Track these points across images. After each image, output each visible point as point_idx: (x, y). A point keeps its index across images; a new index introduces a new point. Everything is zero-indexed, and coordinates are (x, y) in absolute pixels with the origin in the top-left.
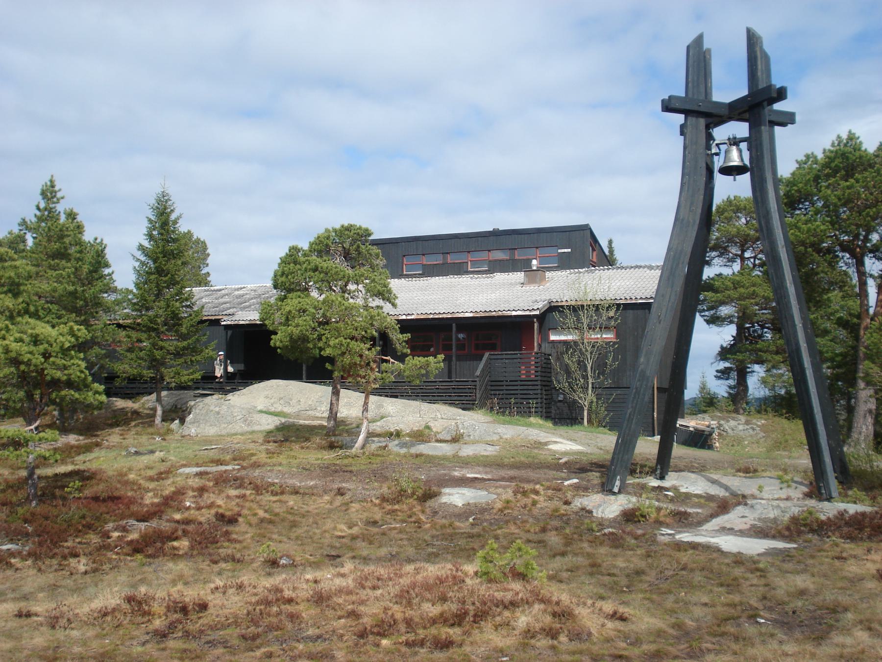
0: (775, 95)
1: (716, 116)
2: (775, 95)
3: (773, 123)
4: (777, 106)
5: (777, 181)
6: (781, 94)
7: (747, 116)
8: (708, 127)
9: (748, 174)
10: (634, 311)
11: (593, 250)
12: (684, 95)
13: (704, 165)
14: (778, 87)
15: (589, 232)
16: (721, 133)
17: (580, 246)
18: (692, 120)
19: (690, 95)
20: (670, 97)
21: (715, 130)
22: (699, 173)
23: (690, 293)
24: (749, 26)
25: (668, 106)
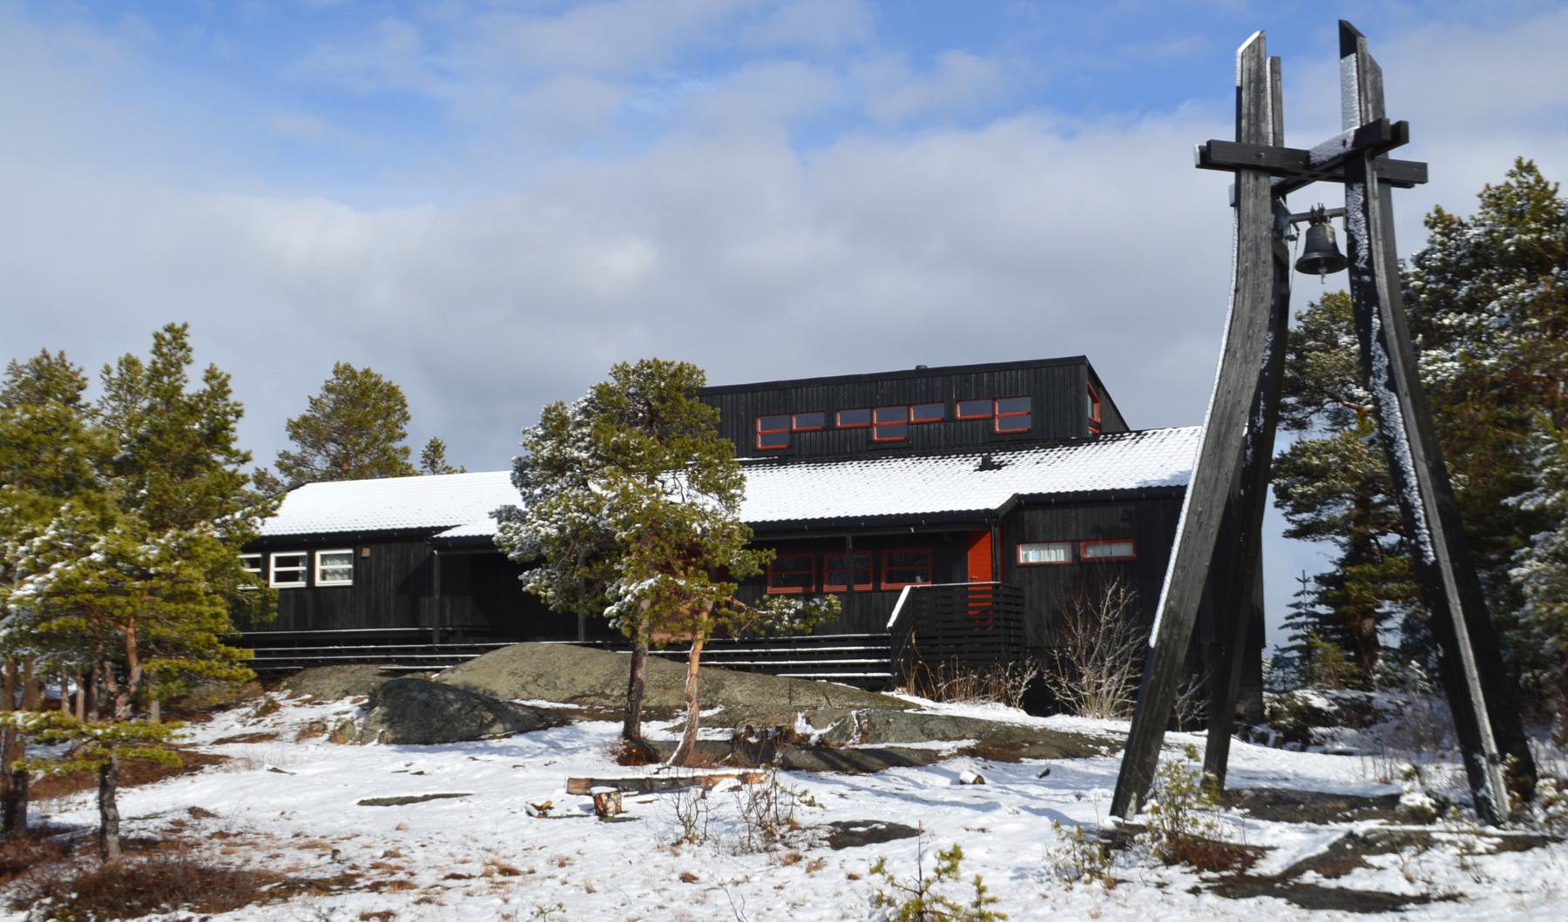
0: (1388, 137)
1: (1301, 169)
2: (1388, 137)
3: (1386, 182)
4: (1395, 154)
5: (1397, 279)
6: (1399, 134)
7: (1341, 172)
8: (1280, 191)
9: (1345, 272)
10: (1155, 504)
11: (1094, 400)
12: (1233, 139)
13: (1270, 257)
14: (1392, 122)
15: (1083, 370)
16: (1300, 201)
17: (1065, 401)
18: (1249, 180)
19: (1244, 141)
20: (1209, 143)
21: (1289, 196)
22: (1266, 265)
23: (1246, 476)
24: (1345, 18)
25: (1209, 158)
